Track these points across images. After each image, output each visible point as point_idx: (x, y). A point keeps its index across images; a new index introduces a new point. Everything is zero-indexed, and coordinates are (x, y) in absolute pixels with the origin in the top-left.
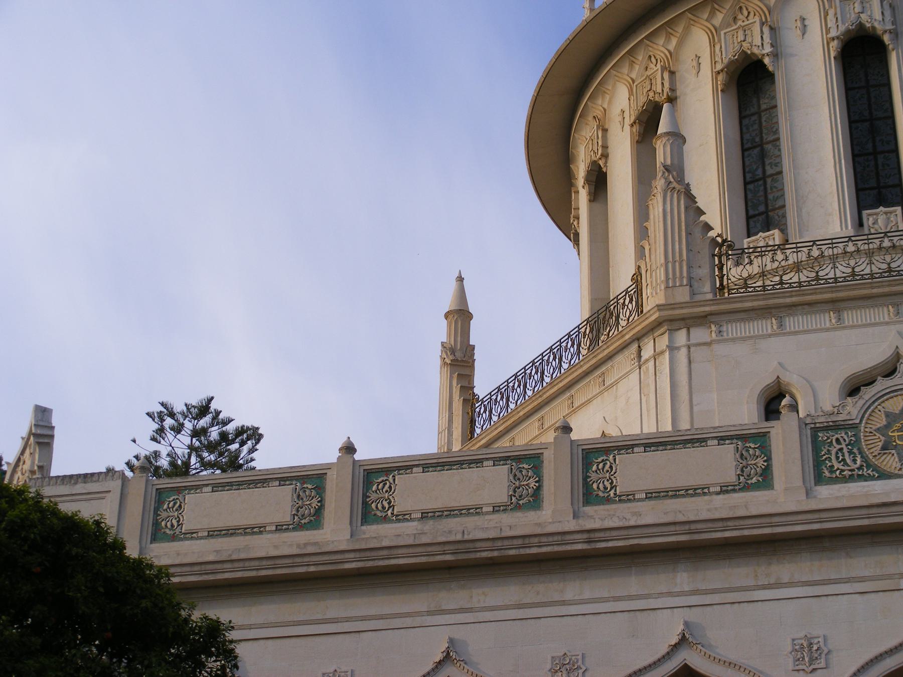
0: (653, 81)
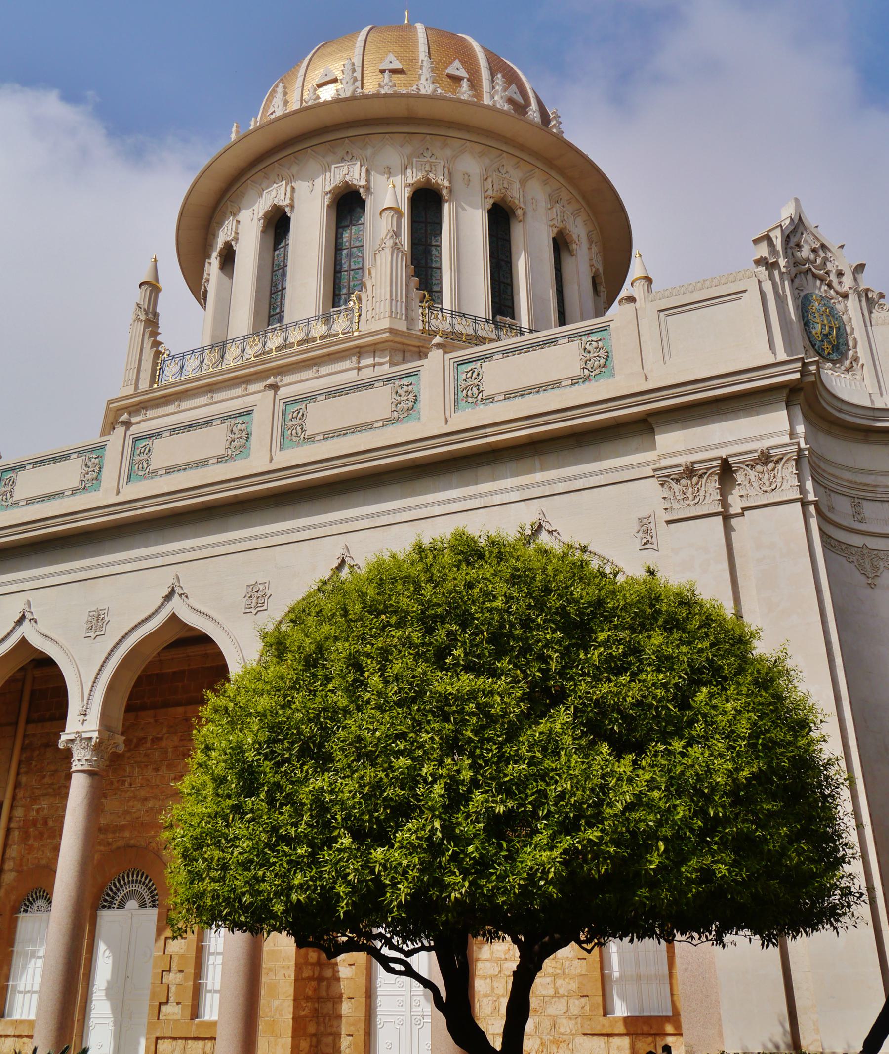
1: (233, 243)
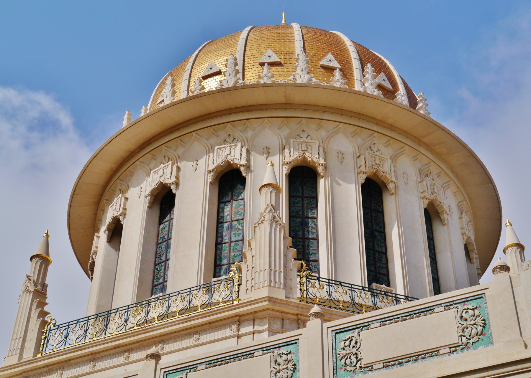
0: (165, 171)
1: (121, 218)
